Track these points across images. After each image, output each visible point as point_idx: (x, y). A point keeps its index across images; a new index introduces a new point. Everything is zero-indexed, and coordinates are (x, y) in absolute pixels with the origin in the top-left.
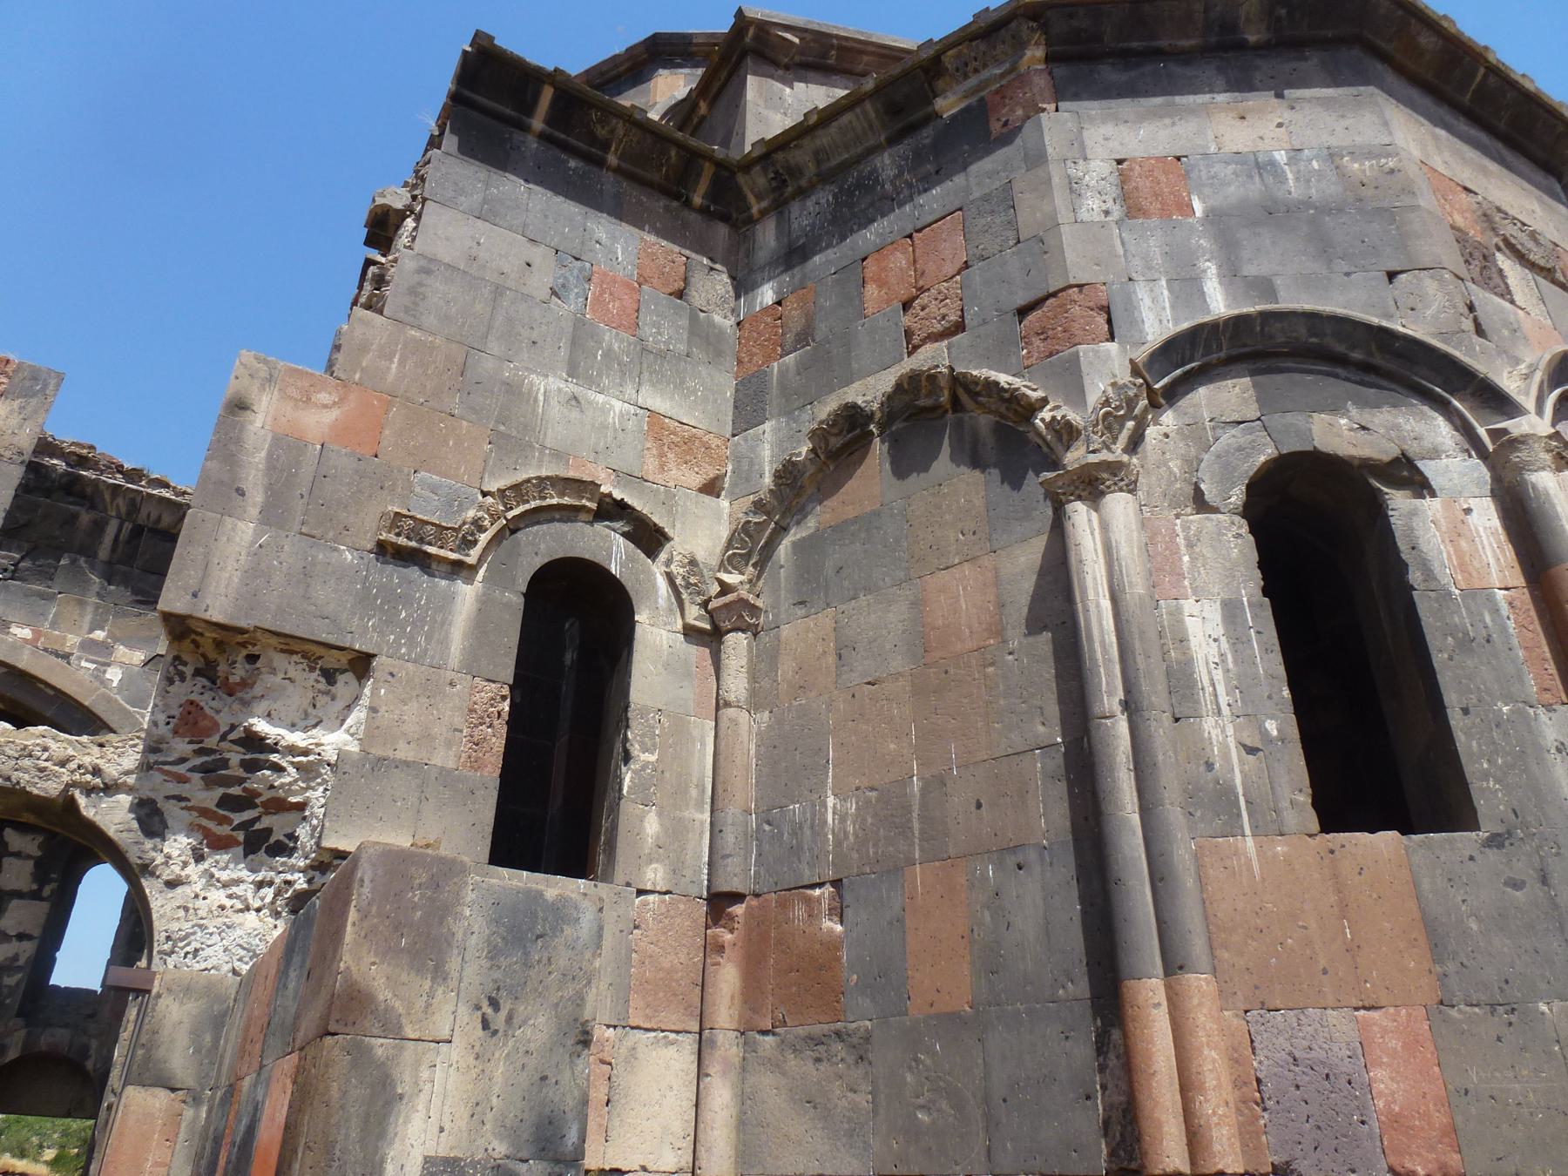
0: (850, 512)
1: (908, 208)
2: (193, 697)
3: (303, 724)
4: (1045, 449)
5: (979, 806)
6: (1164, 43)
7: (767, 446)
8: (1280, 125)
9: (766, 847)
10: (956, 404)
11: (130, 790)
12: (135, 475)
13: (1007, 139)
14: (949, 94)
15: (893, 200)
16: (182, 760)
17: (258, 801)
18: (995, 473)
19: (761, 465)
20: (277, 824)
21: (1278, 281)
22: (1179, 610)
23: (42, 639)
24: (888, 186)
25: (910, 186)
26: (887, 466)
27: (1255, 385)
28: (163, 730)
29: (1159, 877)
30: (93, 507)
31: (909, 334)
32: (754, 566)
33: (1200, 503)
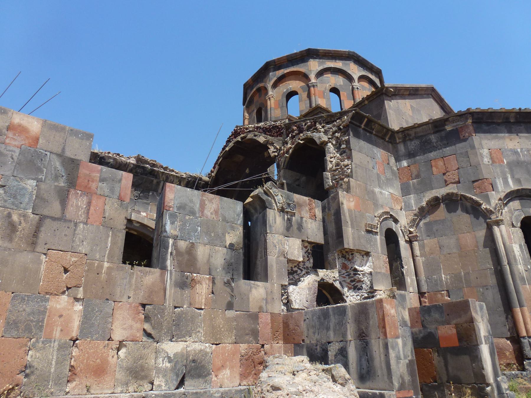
0: (438, 219)
1: (441, 151)
2: (344, 262)
3: (360, 266)
4: (483, 213)
5: (477, 278)
6: (495, 121)
7: (413, 200)
8: (518, 142)
9: (429, 284)
10: (461, 199)
11: (338, 280)
12: (166, 169)
13: (465, 140)
14: (449, 126)
15: (436, 148)
16: (344, 274)
17: (356, 281)
18: (472, 216)
19: (412, 204)
20: (359, 284)
21: (521, 179)
22: (512, 246)
23: (149, 216)
24: (434, 144)
25: (441, 145)
26: (445, 210)
27: (520, 202)
28: (340, 269)
29: (517, 292)
30: (156, 178)
31: (446, 181)
32: (415, 227)
33: (513, 226)
